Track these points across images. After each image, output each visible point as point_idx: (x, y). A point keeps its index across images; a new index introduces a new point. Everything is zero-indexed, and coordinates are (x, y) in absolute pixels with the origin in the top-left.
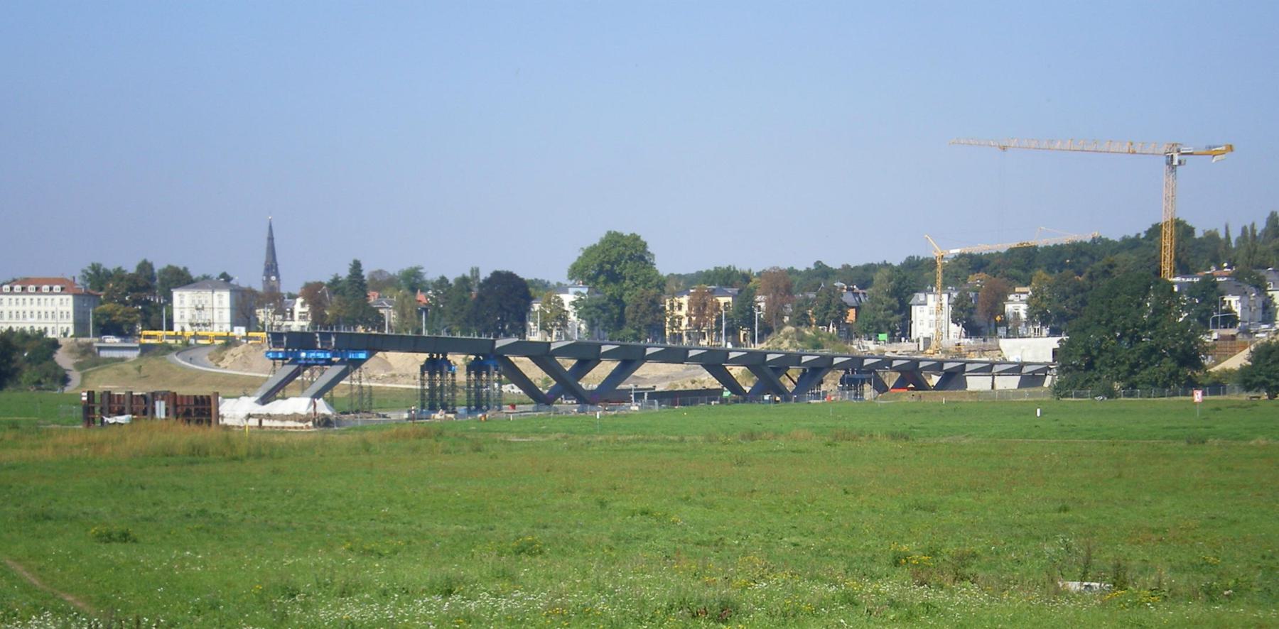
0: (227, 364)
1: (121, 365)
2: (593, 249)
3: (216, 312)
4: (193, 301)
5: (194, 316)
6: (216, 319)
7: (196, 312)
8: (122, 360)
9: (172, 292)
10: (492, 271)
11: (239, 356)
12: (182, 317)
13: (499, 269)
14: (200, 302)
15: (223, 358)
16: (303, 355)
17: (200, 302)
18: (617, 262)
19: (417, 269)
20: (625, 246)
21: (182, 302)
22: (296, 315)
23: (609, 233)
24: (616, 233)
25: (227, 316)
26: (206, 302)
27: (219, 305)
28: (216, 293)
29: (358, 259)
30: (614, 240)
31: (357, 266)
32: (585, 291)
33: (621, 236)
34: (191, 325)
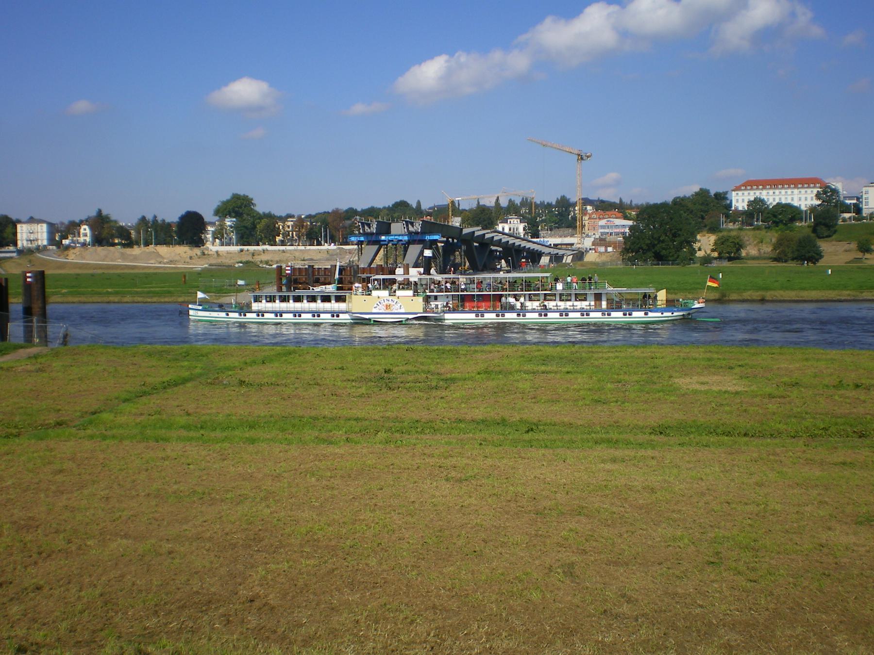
0: (72, 258)
1: (13, 260)
2: (228, 201)
3: (39, 234)
4: (28, 229)
5: (28, 236)
6: (39, 238)
7: (29, 234)
8: (11, 258)
9: (16, 226)
10: (183, 212)
11: (78, 253)
12: (22, 237)
13: (189, 210)
14: (31, 229)
15: (67, 255)
16: (383, 238)
17: (31, 229)
18: (240, 207)
19: (107, 215)
20: (243, 200)
21: (22, 230)
22: (81, 236)
23: (233, 194)
24: (237, 194)
25: (45, 236)
26: (34, 229)
27: (41, 234)
28: (40, 225)
29: (100, 208)
30: (236, 197)
31: (100, 211)
32: (234, 219)
33: (239, 195)
34: (27, 241)
